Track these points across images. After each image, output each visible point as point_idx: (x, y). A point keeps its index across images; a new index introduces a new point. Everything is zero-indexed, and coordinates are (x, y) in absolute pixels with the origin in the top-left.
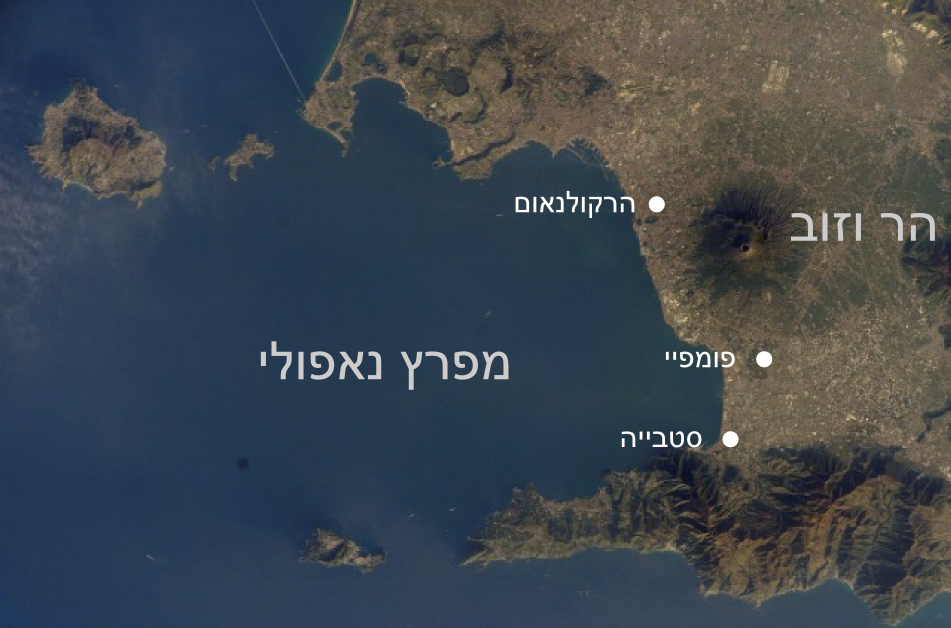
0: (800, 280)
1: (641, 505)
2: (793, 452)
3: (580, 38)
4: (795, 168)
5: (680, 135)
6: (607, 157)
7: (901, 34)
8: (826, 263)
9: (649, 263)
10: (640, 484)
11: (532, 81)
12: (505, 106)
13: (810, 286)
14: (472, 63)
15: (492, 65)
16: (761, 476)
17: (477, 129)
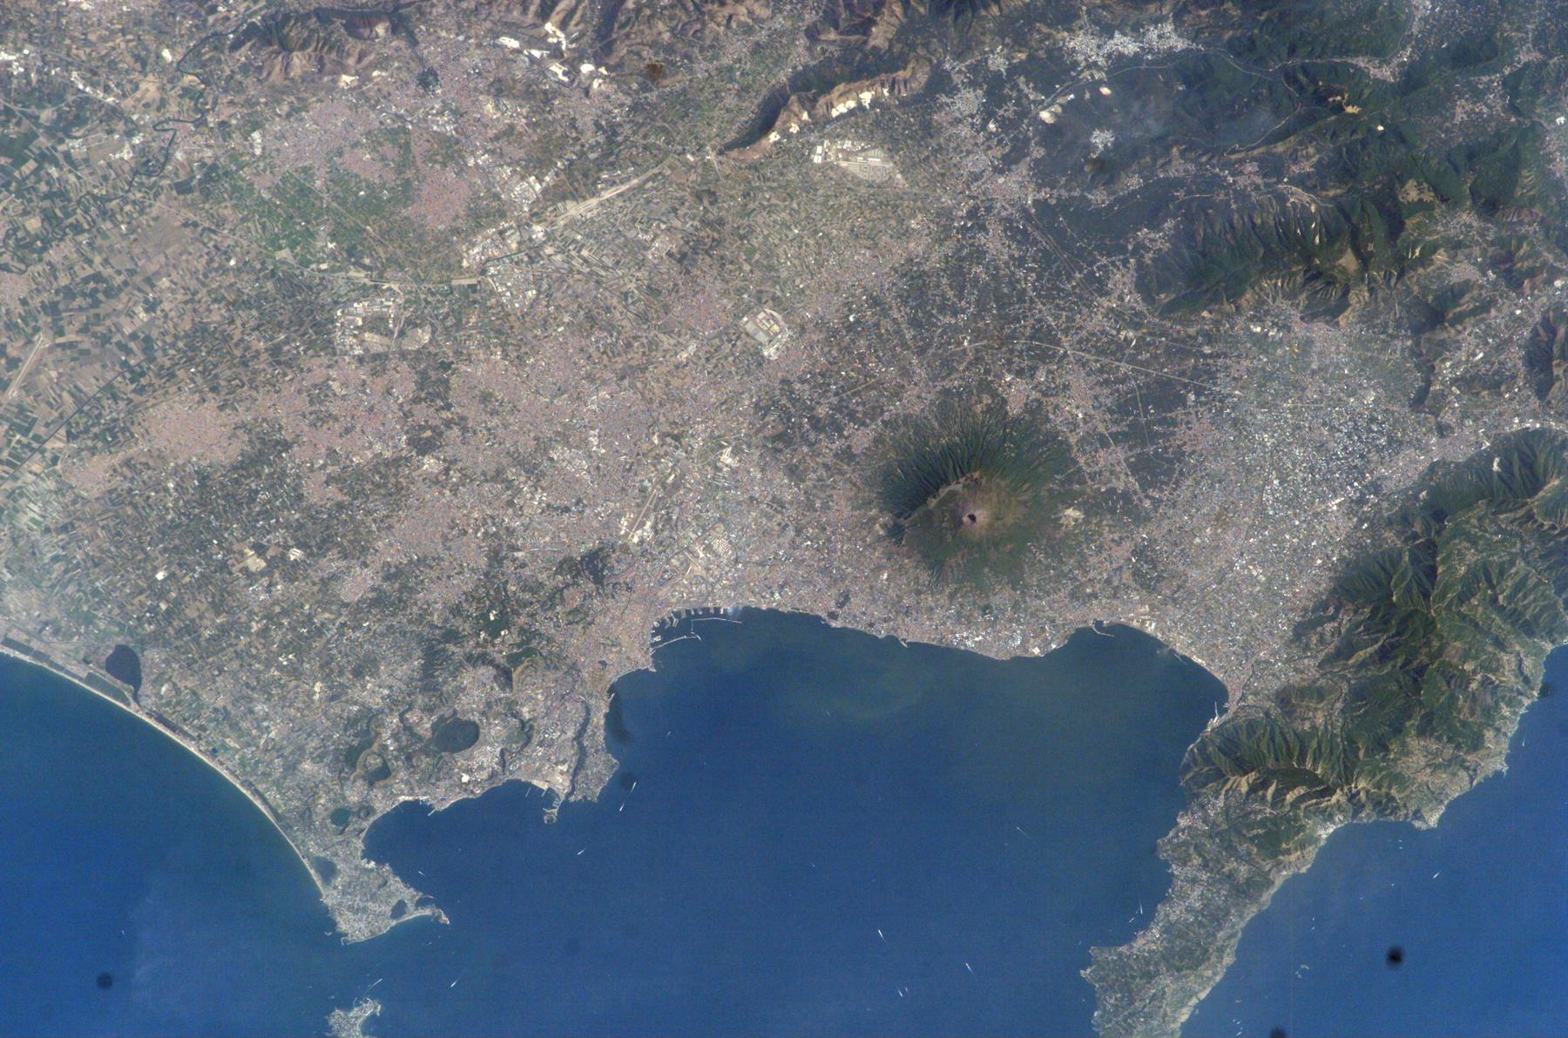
0: (1082, 461)
1: (1235, 839)
2: (1324, 606)
3: (514, 548)
4: (916, 379)
5: (752, 498)
6: (710, 605)
7: (834, 137)
9: (902, 635)
10: (1205, 821)
11: (528, 641)
12: (533, 698)
13: (1102, 453)
14: (443, 699)
15: (466, 679)
16: (1320, 666)
17: (541, 744)
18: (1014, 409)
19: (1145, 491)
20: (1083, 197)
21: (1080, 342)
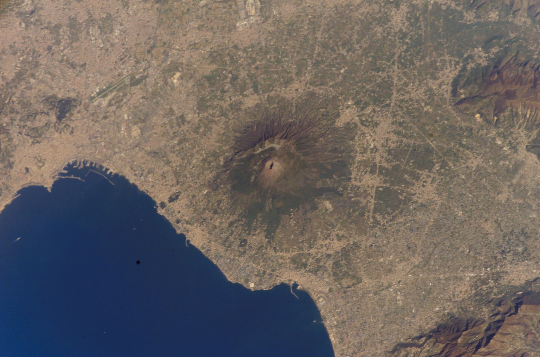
0: (353, 176)
3: (33, 76)
4: (303, 78)
8: (375, 147)
13: (367, 176)
18: (340, 123)
19: (374, 212)
20: (461, 12)
21: (402, 101)
